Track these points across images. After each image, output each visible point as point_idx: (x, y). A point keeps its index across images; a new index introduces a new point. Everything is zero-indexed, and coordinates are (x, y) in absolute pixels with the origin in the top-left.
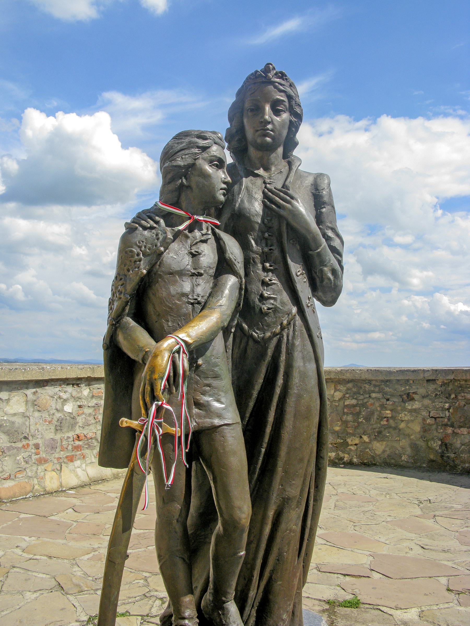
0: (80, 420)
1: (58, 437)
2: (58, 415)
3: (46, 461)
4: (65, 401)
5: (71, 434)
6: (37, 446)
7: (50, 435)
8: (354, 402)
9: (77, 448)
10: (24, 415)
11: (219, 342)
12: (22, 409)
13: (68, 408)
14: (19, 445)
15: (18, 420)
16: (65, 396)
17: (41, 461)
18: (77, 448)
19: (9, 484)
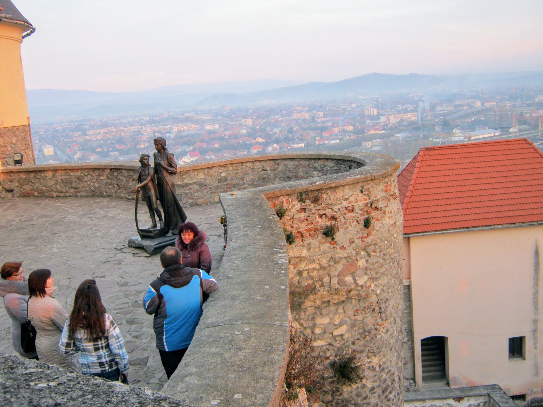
0: (229, 178)
1: (220, 184)
2: (218, 177)
3: (215, 193)
4: (221, 173)
5: (225, 183)
6: (211, 188)
7: (216, 184)
8: (337, 168)
9: (228, 188)
10: (204, 179)
11: (150, 184)
12: (203, 177)
13: (223, 175)
14: (203, 188)
15: (202, 181)
16: (220, 171)
17: (212, 193)
18: (228, 188)
19: (201, 200)
